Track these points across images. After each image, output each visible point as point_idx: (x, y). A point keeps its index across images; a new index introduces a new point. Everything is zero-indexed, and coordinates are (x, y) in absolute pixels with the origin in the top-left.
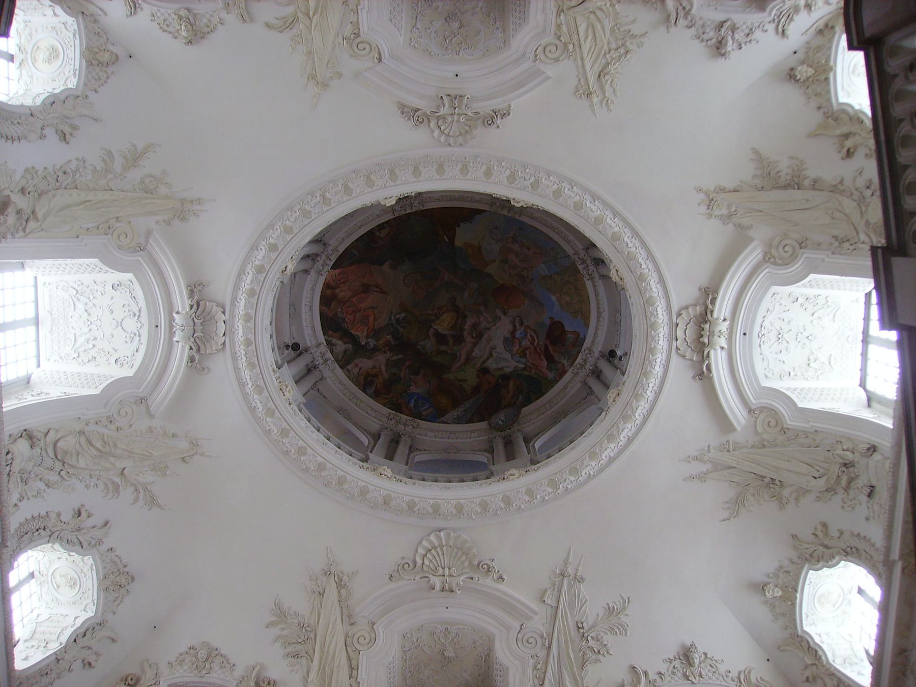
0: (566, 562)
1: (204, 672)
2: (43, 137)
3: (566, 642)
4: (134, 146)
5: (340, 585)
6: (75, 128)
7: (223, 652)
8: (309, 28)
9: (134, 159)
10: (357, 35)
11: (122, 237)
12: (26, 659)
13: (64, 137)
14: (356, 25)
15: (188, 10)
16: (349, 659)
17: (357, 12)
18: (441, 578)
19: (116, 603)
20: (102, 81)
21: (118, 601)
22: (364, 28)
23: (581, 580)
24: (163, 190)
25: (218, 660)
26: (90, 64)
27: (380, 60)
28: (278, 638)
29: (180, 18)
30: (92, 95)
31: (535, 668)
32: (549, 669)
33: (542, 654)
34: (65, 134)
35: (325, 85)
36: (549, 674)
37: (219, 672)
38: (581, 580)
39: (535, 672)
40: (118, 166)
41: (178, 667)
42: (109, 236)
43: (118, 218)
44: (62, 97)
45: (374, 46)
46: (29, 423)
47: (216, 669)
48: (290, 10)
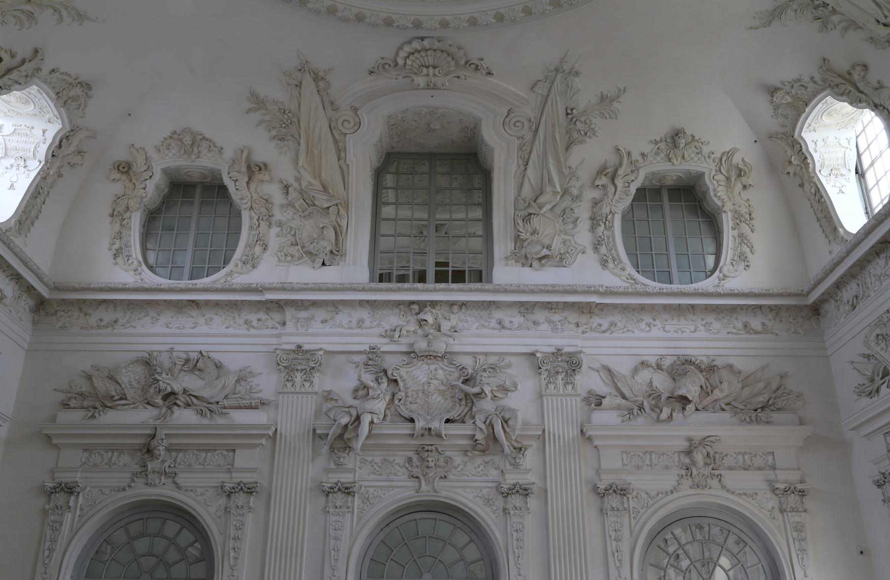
0: (562, 60)
1: (193, 157)
3: (553, 126)
5: (317, 78)
7: (207, 136)
12: (12, 187)
16: (336, 141)
18: (425, 79)
19: (81, 109)
21: (82, 106)
23: (577, 74)
25: (204, 144)
28: (261, 122)
31: (520, 149)
32: (534, 150)
33: (529, 136)
36: (534, 156)
37: (209, 155)
38: (577, 74)
39: (520, 153)
41: (166, 152)
47: (205, 152)
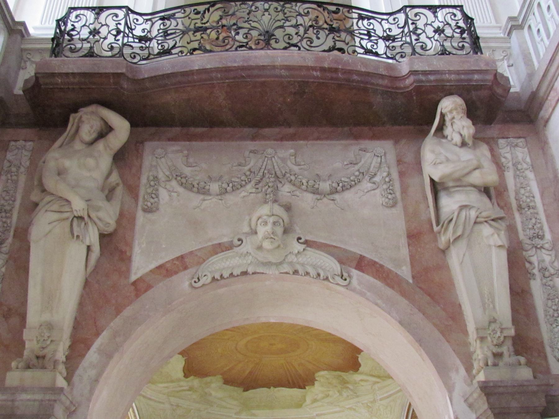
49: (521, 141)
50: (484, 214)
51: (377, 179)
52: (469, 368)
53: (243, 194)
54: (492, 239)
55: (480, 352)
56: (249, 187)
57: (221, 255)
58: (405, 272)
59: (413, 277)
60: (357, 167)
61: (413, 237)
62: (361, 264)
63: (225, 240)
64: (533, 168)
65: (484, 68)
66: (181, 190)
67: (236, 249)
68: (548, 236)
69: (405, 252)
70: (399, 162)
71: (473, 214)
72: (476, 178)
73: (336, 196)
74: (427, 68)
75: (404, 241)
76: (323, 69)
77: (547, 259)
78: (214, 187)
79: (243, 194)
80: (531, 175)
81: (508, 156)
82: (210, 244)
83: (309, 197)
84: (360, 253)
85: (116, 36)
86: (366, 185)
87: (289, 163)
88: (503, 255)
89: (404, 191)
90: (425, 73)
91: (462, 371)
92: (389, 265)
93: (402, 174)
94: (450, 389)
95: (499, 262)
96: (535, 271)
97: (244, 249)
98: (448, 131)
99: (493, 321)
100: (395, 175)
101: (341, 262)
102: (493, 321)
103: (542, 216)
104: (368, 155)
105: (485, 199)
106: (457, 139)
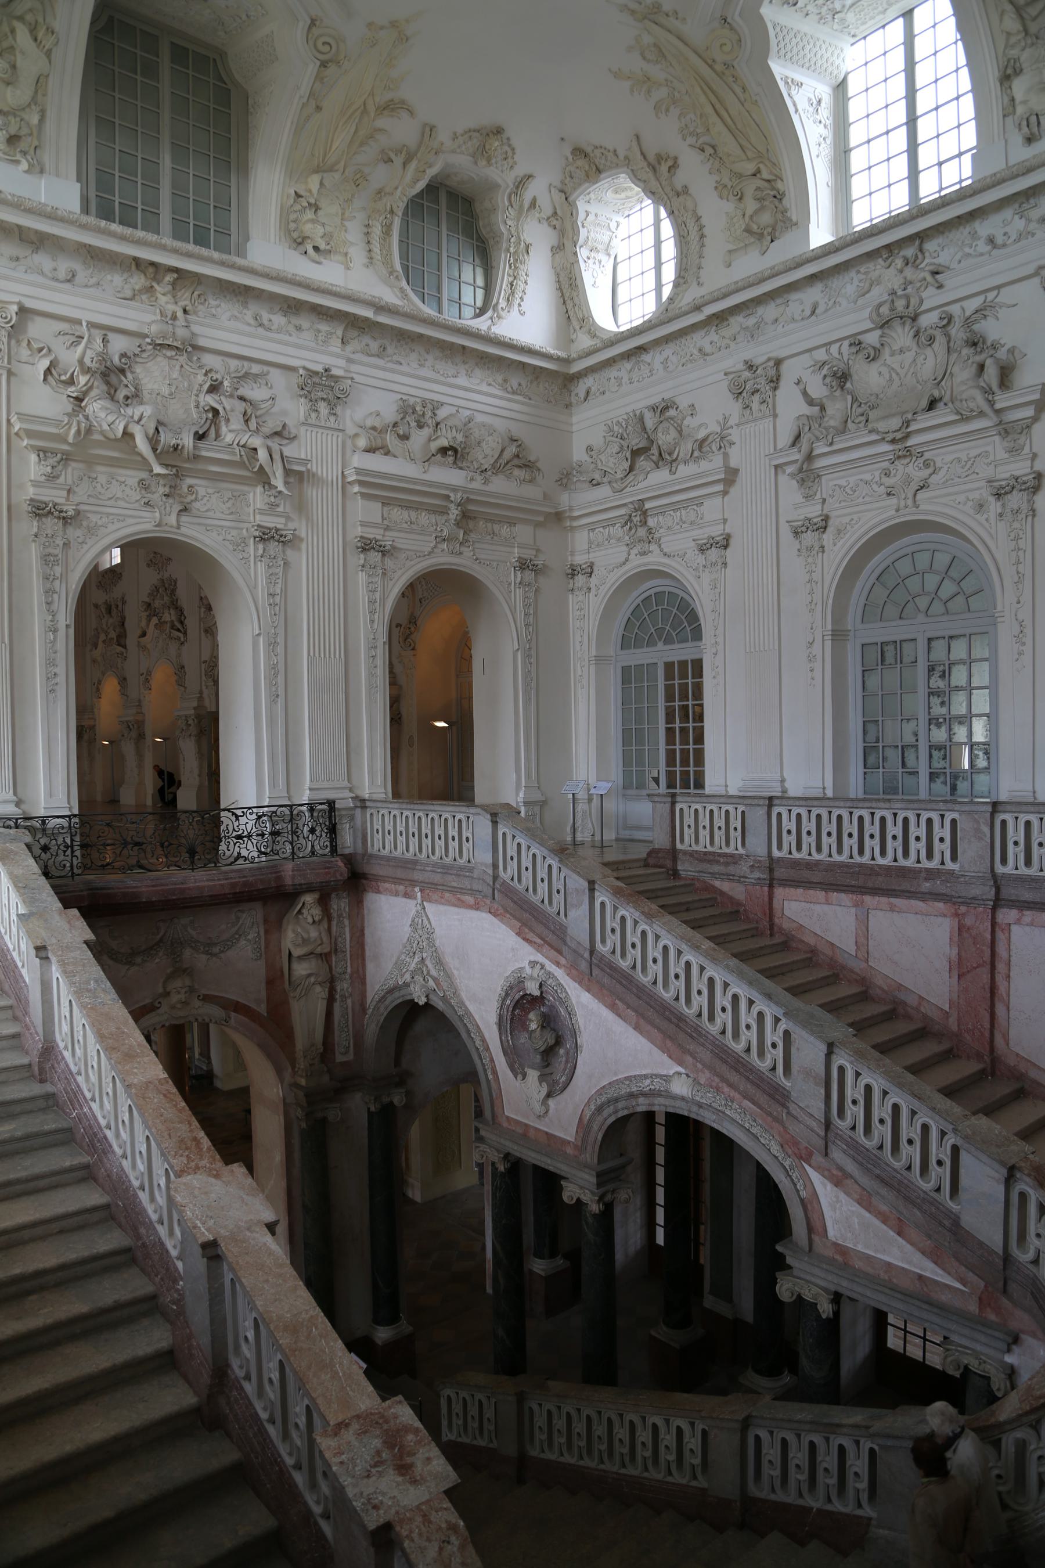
2: (686, 190)
4: (632, 91)
6: (659, 158)
8: (372, 94)
9: (645, 83)
10: (324, 64)
11: (727, 48)
13: (673, 167)
14: (319, 78)
15: (476, 163)
17: (312, 94)
20: (603, 151)
22: (312, 68)
24: (647, 39)
26: (599, 171)
27: (313, 22)
29: (489, 160)
30: (621, 154)
34: (670, 168)
35: (393, 24)
40: (663, 92)
42: (735, 64)
43: (710, 66)
44: (642, 184)
45: (311, 42)
46: (993, 74)
48: (380, 123)
49: (345, 895)
50: (319, 979)
51: (249, 937)
52: (293, 1067)
53: (157, 960)
54: (320, 993)
55: (302, 1064)
56: (161, 954)
57: (147, 1017)
58: (263, 1009)
59: (268, 1013)
60: (236, 928)
61: (270, 983)
62: (238, 1007)
63: (147, 1001)
64: (350, 917)
65: (339, 878)
66: (111, 962)
67: (158, 1011)
68: (349, 970)
69: (264, 993)
70: (266, 921)
71: (313, 979)
72: (319, 950)
73: (222, 955)
74: (303, 882)
75: (263, 986)
76: (235, 893)
77: (346, 986)
78: (139, 960)
79: (157, 960)
80: (346, 922)
81: (335, 907)
82: (137, 1006)
83: (204, 957)
84: (235, 998)
85: (65, 852)
86: (243, 942)
87: (189, 929)
88: (325, 1002)
89: (266, 947)
90: (301, 885)
91: (290, 1070)
92: (253, 1006)
93: (266, 932)
94: (282, 1081)
95: (321, 1007)
96: (337, 997)
97: (161, 1011)
98: (304, 911)
99: (313, 1045)
100: (262, 933)
101: (224, 1008)
102: (313, 1045)
103: (348, 956)
104: (244, 915)
105: (320, 961)
106: (310, 920)
